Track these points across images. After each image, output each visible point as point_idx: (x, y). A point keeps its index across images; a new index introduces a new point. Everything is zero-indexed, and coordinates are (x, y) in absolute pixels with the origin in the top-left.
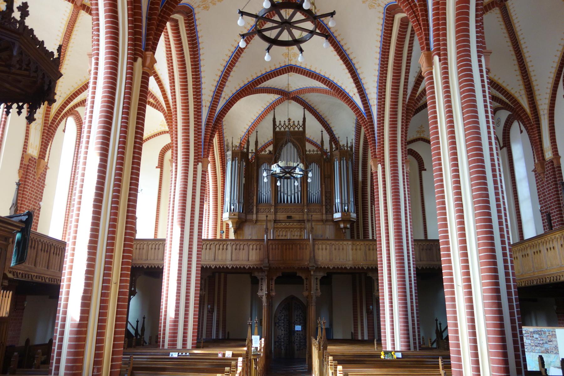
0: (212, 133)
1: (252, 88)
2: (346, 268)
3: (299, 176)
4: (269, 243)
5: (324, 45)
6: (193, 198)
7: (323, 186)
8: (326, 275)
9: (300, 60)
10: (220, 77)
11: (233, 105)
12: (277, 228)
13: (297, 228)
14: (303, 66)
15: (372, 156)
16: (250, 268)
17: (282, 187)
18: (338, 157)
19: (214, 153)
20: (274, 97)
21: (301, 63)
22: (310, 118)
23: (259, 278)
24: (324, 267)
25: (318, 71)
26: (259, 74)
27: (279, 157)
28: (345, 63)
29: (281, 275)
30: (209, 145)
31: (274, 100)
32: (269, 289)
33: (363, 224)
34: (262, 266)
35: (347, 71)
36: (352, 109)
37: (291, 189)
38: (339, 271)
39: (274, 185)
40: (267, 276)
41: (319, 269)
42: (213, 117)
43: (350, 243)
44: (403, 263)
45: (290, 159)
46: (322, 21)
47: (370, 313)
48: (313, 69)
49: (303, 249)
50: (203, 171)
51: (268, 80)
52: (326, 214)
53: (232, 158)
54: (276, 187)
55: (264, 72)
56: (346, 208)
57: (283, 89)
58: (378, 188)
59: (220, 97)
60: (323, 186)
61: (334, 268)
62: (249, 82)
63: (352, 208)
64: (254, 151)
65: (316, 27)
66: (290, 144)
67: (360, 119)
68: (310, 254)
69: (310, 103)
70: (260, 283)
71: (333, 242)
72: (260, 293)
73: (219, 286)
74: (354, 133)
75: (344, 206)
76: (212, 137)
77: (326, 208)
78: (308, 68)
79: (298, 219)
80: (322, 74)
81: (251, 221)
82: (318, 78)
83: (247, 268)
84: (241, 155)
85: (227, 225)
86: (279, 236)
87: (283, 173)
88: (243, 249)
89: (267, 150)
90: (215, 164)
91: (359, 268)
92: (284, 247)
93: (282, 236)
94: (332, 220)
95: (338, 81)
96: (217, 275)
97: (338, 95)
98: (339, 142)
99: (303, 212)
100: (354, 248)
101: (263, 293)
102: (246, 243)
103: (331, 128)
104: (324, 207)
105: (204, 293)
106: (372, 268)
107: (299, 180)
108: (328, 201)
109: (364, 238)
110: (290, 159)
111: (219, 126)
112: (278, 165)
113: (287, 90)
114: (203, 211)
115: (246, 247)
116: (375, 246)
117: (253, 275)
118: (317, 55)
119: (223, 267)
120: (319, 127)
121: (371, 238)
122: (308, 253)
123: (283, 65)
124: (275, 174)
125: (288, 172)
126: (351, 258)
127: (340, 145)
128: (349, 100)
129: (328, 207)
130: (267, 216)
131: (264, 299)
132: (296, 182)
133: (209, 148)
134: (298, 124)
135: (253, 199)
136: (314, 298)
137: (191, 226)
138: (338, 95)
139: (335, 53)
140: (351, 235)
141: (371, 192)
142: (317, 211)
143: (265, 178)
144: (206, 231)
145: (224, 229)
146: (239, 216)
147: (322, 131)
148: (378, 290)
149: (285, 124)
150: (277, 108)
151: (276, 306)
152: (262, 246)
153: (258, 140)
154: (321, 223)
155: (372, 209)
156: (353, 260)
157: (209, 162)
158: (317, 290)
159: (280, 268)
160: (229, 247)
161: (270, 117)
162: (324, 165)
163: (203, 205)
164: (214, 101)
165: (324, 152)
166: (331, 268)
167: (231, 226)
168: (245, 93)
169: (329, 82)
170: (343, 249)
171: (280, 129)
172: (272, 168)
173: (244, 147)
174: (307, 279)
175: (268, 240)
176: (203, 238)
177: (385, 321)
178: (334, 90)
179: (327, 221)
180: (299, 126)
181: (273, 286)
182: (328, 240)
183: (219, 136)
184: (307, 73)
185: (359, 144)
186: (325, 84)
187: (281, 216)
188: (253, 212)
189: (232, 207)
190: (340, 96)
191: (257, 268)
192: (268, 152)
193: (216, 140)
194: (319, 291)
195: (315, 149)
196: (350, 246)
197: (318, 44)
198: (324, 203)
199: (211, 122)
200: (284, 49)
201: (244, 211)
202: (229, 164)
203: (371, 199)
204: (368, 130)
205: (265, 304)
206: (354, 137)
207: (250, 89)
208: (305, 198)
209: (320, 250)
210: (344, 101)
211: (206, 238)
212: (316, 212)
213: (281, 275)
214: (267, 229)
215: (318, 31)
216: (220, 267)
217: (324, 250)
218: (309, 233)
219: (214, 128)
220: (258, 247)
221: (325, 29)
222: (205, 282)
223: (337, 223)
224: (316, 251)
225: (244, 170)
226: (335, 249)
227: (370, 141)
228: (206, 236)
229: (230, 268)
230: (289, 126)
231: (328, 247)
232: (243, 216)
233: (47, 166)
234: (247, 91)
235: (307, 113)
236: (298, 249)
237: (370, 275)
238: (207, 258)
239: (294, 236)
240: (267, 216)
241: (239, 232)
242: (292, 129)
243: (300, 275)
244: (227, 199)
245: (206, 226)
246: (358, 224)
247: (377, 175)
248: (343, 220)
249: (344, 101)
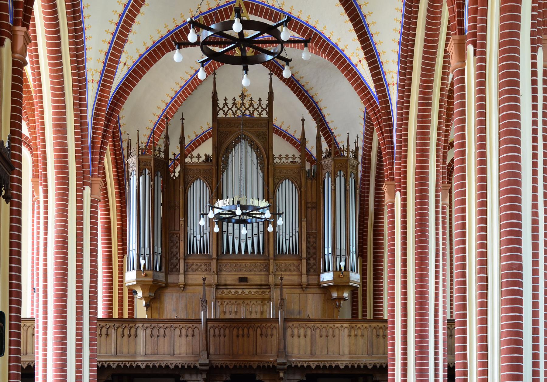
2: (337, 367)
4: (209, 325)
7: (304, 223)
8: (305, 379)
10: (118, 25)
12: (222, 299)
16: (176, 367)
34: (197, 364)
38: (327, 372)
52: (307, 275)
56: (343, 264)
60: (304, 223)
62: (170, 32)
71: (318, 324)
75: (338, 260)
77: (308, 264)
79: (259, 282)
81: (176, 285)
88: (165, 336)
91: (359, 366)
92: (235, 332)
93: (230, 312)
94: (319, 285)
99: (267, 269)
104: (304, 261)
108: (312, 251)
129: (312, 261)
130: (204, 279)
135: (178, 247)
142: (292, 268)
154: (298, 290)
160: (140, 332)
175: (208, 320)
179: (308, 285)
182: (309, 320)
187: (230, 278)
188: (178, 270)
189: (142, 262)
196: (346, 331)
198: (304, 255)
202: (134, 180)
209: (296, 338)
212: (290, 271)
217: (302, 337)
220: (190, 332)
223: (326, 289)
224: (289, 339)
226: (321, 336)
231: (309, 332)
232: (161, 277)
239: (251, 312)
241: (154, 305)
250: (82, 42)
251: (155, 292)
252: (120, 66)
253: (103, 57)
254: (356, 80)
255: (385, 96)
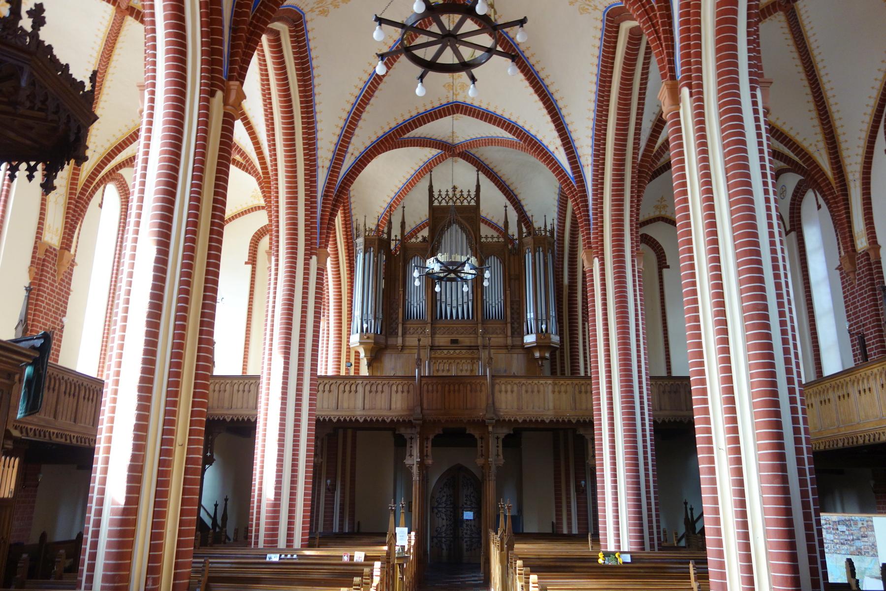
0: (333, 210)
1: (396, 138)
2: (543, 421)
3: (470, 277)
4: (423, 382)
5: (509, 71)
6: (303, 312)
7: (508, 292)
8: (512, 432)
9: (471, 94)
11: (366, 165)
12: (435, 358)
13: (466, 358)
14: (476, 104)
15: (585, 245)
17: (443, 293)
18: (531, 246)
19: (336, 240)
20: (430, 153)
21: (473, 99)
22: (487, 185)
23: (407, 437)
24: (510, 420)
25: (499, 112)
26: (407, 117)
27: (438, 247)
28: (542, 99)
29: (441, 432)
30: (328, 228)
31: (430, 156)
32: (422, 455)
33: (571, 352)
34: (412, 419)
35: (545, 111)
36: (553, 172)
37: (457, 298)
38: (533, 426)
39: (430, 291)
40: (420, 434)
41: (501, 423)
42: (335, 185)
43: (549, 382)
44: (634, 413)
45: (456, 250)
46: (507, 33)
47: (581, 492)
48: (492, 109)
49: (476, 391)
50: (318, 269)
51: (421, 125)
52: (512, 337)
53: (365, 248)
54: (434, 293)
55: (414, 113)
56: (544, 327)
57: (444, 140)
58: (593, 296)
59: (346, 152)
60: (508, 292)
61: (525, 421)
63: (553, 328)
64: (399, 237)
65: (496, 43)
66: (455, 227)
67: (565, 186)
68: (487, 399)
69: (487, 162)
70: (408, 445)
71: (523, 381)
72: (408, 461)
73: (344, 449)
74: (556, 209)
75: (540, 323)
76: (333, 215)
77: (512, 328)
78: (484, 106)
79: (468, 344)
80: (506, 116)
81: (395, 347)
82: (500, 122)
83: (388, 421)
84: (379, 243)
85: (357, 353)
86: (438, 371)
87: (444, 271)
89: (420, 235)
90: (338, 257)
92: (447, 389)
93: (443, 370)
94: (522, 346)
95: (531, 127)
96: (341, 432)
97: (531, 149)
98: (532, 223)
99: (476, 333)
100: (556, 390)
101: (413, 460)
102: (386, 382)
103: (519, 201)
104: (509, 325)
105: (320, 460)
106: (585, 421)
107: (470, 283)
108: (515, 316)
109: (572, 374)
110: (456, 250)
111: (343, 199)
112: (437, 259)
113: (450, 141)
114: (319, 332)
115: (386, 388)
116: (589, 387)
117: (397, 432)
118: (499, 86)
119: (351, 420)
120: (502, 199)
121: (582, 374)
122: (484, 398)
123: (444, 102)
124: (433, 273)
125: (452, 270)
126: (551, 406)
127: (534, 229)
128: (548, 158)
129: (516, 325)
130: (419, 340)
131: (415, 470)
132: (465, 286)
133: (328, 233)
134: (469, 195)
135: (398, 313)
136: (493, 468)
137: (300, 355)
138: (531, 149)
139: (527, 83)
140: (552, 369)
141: (583, 302)
142: (498, 331)
143: (417, 280)
144: (324, 363)
145: (353, 361)
146: (375, 339)
147: (506, 207)
148: (594, 456)
149: (447, 195)
150: (435, 170)
151: (434, 480)
152: (411, 387)
153: (406, 220)
154: (505, 351)
155: (584, 328)
156: (554, 408)
157: (328, 255)
158: (498, 455)
159: (439, 421)
161: (424, 184)
162: (509, 260)
163: (319, 323)
164: (336, 159)
165: (509, 239)
166: (520, 421)
167: (362, 354)
168: (386, 147)
169: (517, 128)
170: (539, 392)
171: (440, 203)
172: (428, 265)
173: (383, 232)
174: (482, 438)
175: (421, 377)
176: (319, 374)
177: (604, 505)
178: (525, 142)
179: (513, 347)
180: (469, 199)
181: (429, 449)
182: (515, 377)
183: (345, 213)
184: (482, 115)
185: (564, 227)
186: (510, 132)
187: (442, 340)
188: (397, 334)
189: (365, 326)
190: (535, 152)
191: (404, 421)
192: (420, 239)
193: (339, 221)
194: (501, 457)
195: (495, 234)
196: (550, 387)
197: (500, 68)
198: (509, 320)
199: (332, 192)
200: (446, 77)
201: (383, 332)
202: (360, 257)
203: (583, 313)
204: (577, 204)
205: (416, 477)
206: (555, 216)
207: (392, 140)
208: (478, 312)
209: (503, 394)
210: (541, 158)
211: (323, 374)
212: (497, 333)
213: (441, 432)
214: (419, 359)
215: (499, 48)
216: (345, 420)
217: (509, 393)
218: (485, 366)
219: (336, 200)
220: (406, 388)
221: (511, 46)
222: (322, 443)
223: (529, 350)
224: (497, 394)
225: (383, 267)
226: (527, 392)
227: (581, 222)
228: (324, 370)
229: (361, 421)
230: (455, 199)
231: (515, 388)
232: (382, 340)
233: (73, 261)
234: (389, 143)
235: (483, 177)
236: (468, 392)
237: (581, 431)
238: (325, 406)
239: (462, 370)
240: (419, 340)
241: (375, 365)
242: (458, 203)
243: (472, 432)
244: (357, 313)
245: (324, 356)
246: (562, 353)
247: (592, 276)
248: (539, 346)
249: (541, 158)
250: (314, 133)
251: (377, 351)
252: (348, 156)
253: (333, 147)
254: (554, 165)
255: (580, 176)
